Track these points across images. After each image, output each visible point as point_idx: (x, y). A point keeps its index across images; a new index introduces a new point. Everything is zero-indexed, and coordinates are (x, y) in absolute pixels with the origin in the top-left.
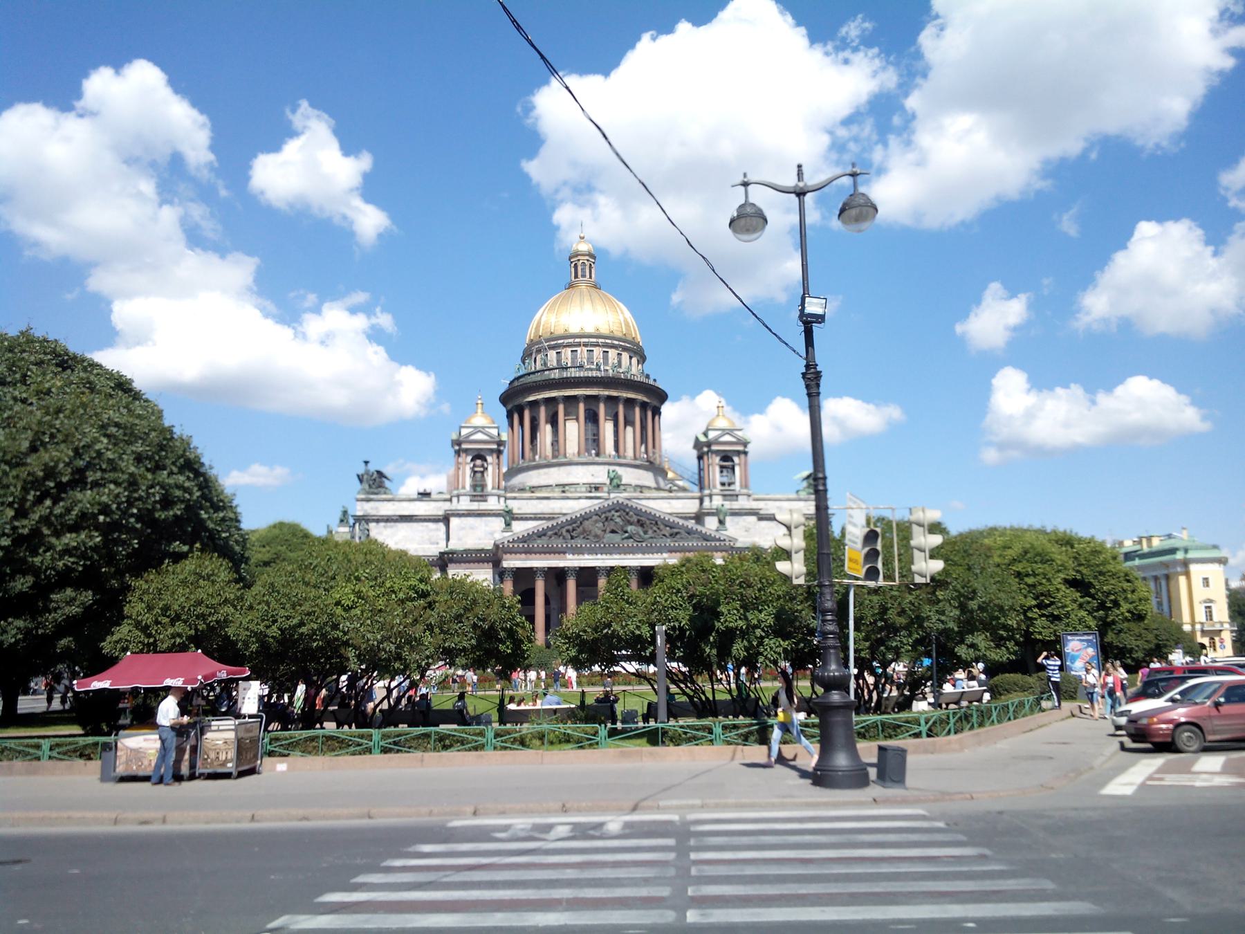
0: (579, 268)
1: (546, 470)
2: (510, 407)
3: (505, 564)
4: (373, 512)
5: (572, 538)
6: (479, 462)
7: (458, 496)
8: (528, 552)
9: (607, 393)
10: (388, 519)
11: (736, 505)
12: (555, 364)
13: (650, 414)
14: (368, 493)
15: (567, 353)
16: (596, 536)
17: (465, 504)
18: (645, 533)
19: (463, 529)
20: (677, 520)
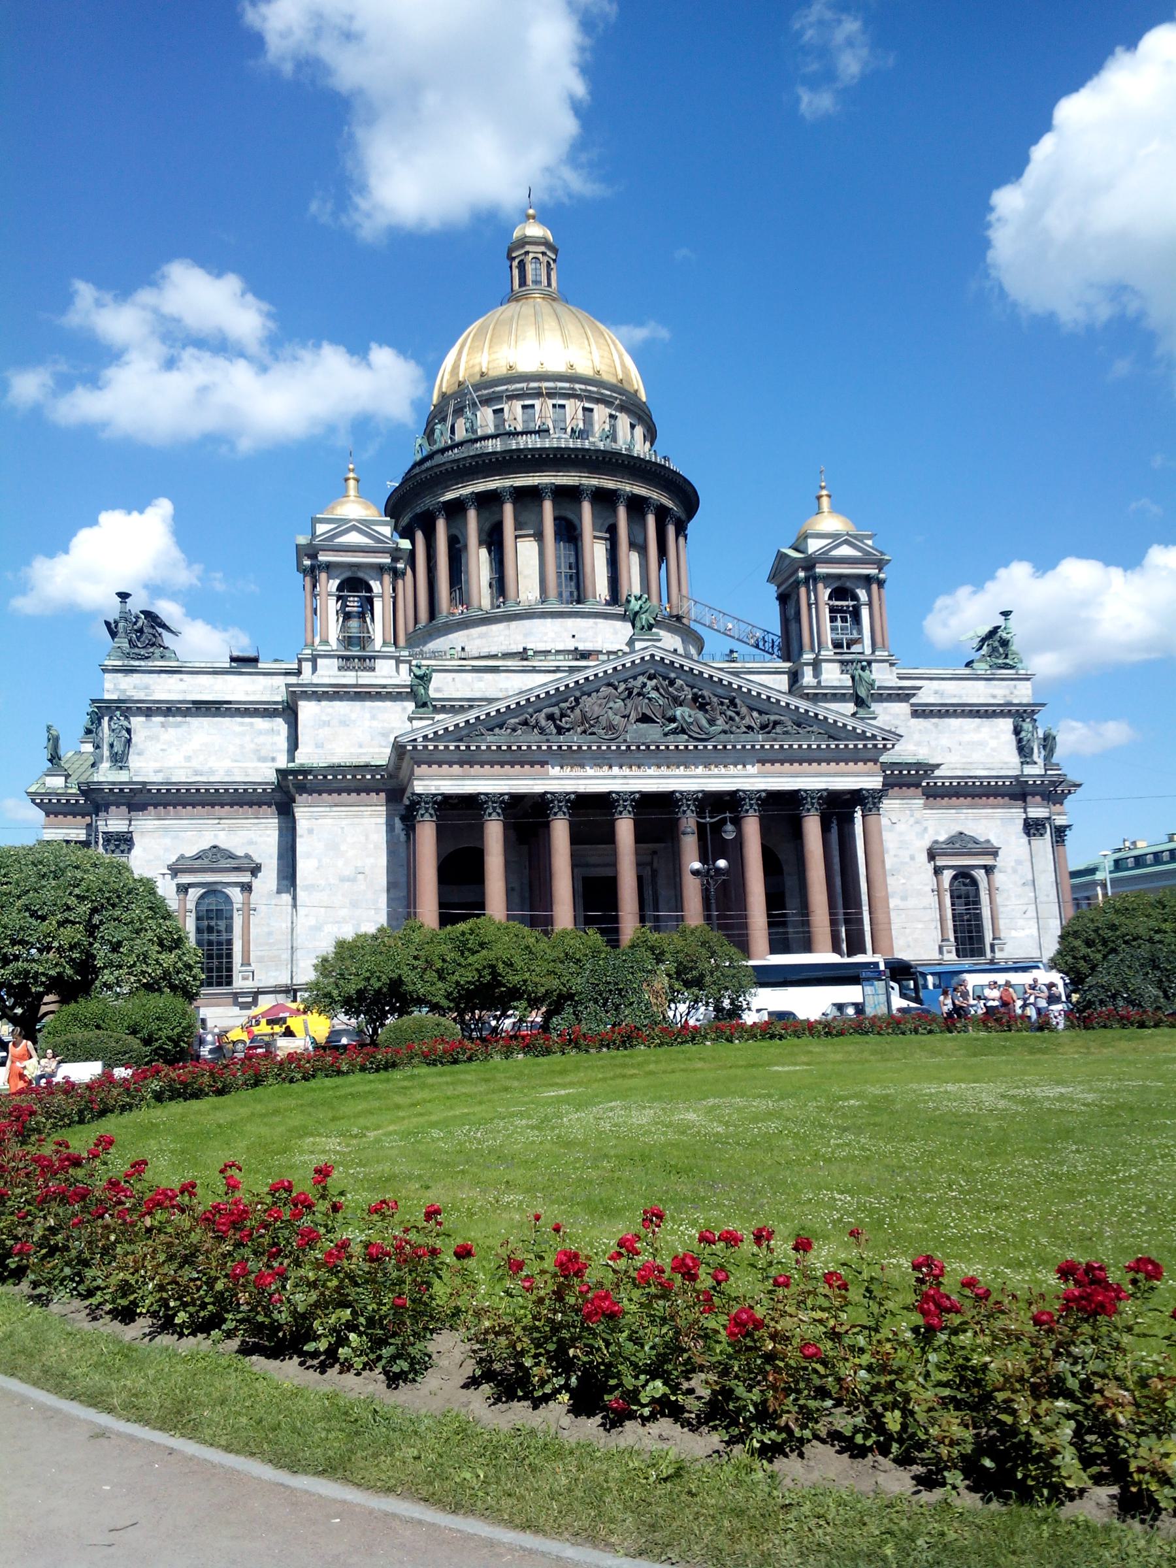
0: (530, 268)
1: (483, 629)
2: (405, 521)
3: (419, 787)
4: (141, 695)
5: (560, 731)
7: (314, 660)
8: (468, 760)
9: (595, 482)
10: (170, 710)
12: (491, 430)
13: (671, 530)
14: (128, 656)
15: (514, 412)
16: (611, 727)
17: (328, 673)
18: (712, 722)
19: (327, 724)
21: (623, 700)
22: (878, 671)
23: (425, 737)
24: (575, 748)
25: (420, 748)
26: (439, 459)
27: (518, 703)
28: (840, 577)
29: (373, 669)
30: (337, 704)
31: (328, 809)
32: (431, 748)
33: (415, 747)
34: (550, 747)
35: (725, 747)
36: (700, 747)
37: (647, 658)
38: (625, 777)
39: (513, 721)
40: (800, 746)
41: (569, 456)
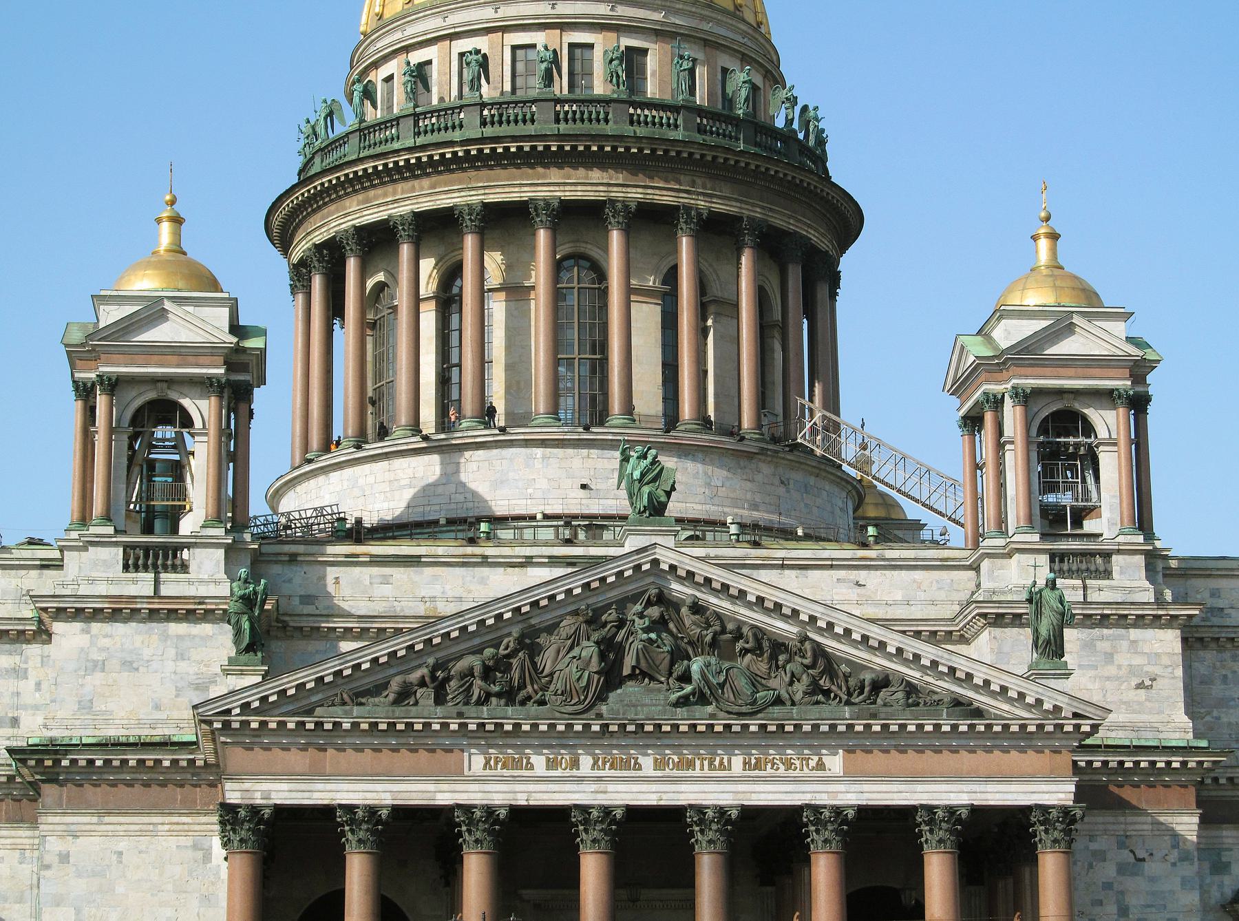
3: (234, 793)
6: (164, 432)
9: (636, 194)
11: (1102, 592)
19: (99, 666)
20: (876, 633)
21: (597, 643)
22: (1121, 573)
23: (245, 707)
24: (508, 728)
25: (236, 725)
26: (351, 150)
27: (412, 647)
28: (1060, 392)
29: (184, 567)
30: (119, 629)
31: (95, 819)
32: (254, 725)
33: (227, 725)
34: (463, 726)
35: (781, 727)
36: (736, 729)
37: (646, 567)
38: (599, 779)
39: (399, 679)
40: (920, 727)
41: (588, 148)
